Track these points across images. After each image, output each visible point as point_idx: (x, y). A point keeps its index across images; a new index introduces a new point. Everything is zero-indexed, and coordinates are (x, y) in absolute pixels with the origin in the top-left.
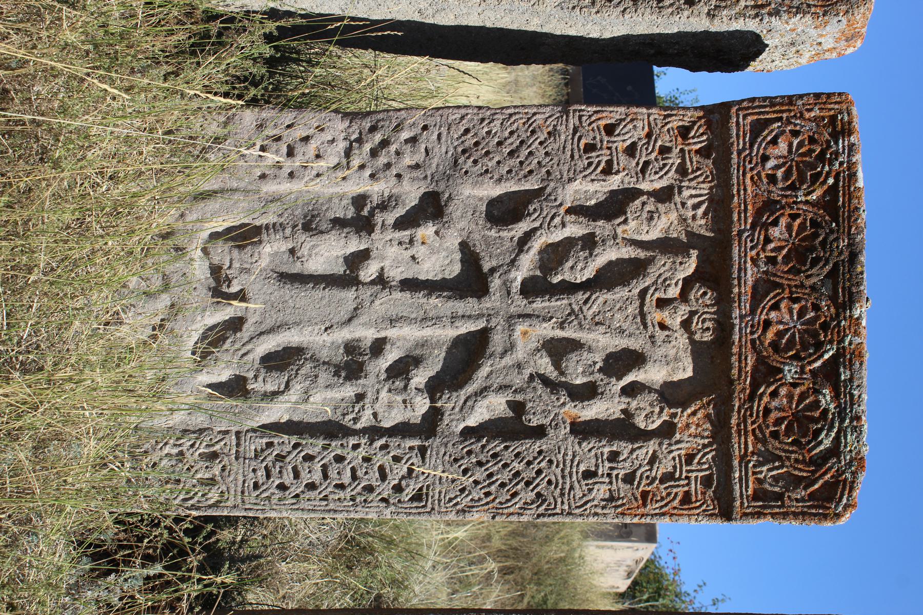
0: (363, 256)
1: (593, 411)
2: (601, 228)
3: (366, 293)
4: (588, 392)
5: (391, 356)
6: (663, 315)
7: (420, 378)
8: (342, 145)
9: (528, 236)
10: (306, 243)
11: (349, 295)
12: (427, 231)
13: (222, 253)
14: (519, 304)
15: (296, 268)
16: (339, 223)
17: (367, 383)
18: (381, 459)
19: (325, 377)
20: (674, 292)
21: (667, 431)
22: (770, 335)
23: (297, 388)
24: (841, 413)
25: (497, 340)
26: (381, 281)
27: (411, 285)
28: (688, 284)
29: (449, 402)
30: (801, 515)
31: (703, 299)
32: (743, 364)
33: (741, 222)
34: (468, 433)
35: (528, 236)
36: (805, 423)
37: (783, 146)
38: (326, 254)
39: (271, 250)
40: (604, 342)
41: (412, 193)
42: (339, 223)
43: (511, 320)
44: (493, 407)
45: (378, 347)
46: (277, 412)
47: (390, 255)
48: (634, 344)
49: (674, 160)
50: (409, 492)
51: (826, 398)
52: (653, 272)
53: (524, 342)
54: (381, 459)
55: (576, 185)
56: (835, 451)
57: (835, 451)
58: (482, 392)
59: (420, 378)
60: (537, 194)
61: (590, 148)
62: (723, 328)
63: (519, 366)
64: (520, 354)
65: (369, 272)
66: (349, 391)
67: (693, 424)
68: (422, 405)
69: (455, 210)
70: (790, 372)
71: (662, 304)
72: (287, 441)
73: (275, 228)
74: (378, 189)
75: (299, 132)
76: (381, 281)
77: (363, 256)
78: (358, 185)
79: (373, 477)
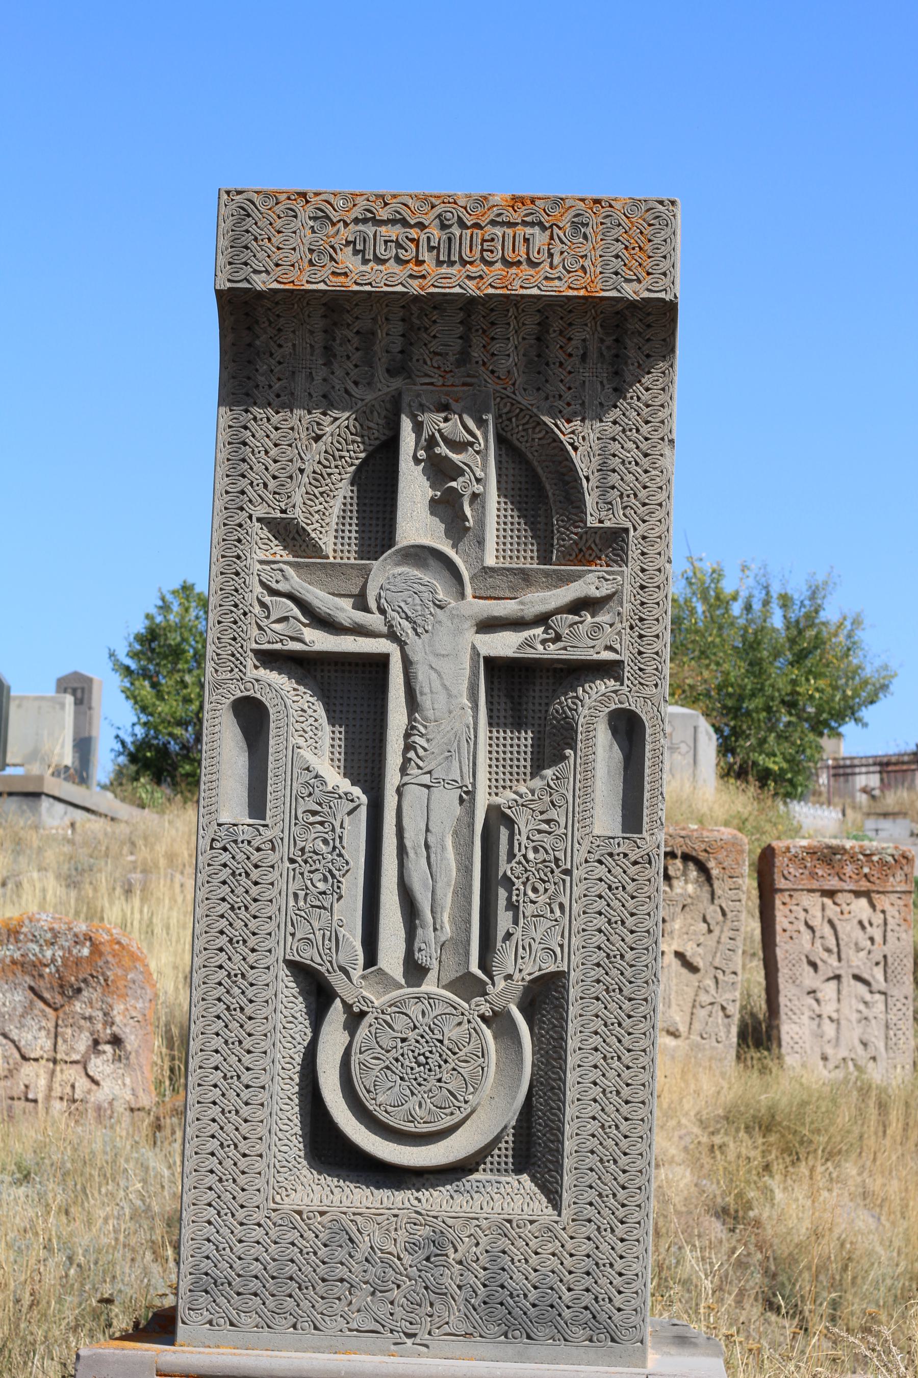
0: (830, 1018)
1: (878, 938)
2: (818, 934)
3: (842, 1017)
4: (872, 939)
5: (862, 1007)
6: (845, 912)
7: (868, 997)
8: (793, 1026)
9: (822, 960)
10: (826, 1038)
11: (843, 1022)
12: (819, 995)
13: (831, 1065)
14: (844, 963)
15: (834, 1041)
16: (819, 1026)
17: (871, 1016)
18: (895, 1009)
19: (869, 1030)
20: (838, 909)
21: (883, 912)
22: (854, 876)
23: (873, 1039)
24: (880, 853)
25: (856, 971)
26: (838, 1011)
27: (839, 1000)
28: (835, 903)
29: (875, 987)
30: (912, 867)
31: (840, 898)
32: (864, 885)
33: (815, 885)
34: (886, 980)
35: (822, 960)
36: (883, 863)
37: (791, 870)
38: (829, 1029)
39: (829, 1051)
40: (858, 934)
41: (810, 1001)
42: (819, 1026)
43: (850, 967)
44: (878, 973)
45: (860, 1012)
46: (881, 1045)
47: (829, 1009)
48: (855, 922)
49: (794, 908)
50: (904, 1001)
51: (875, 858)
52: (832, 916)
53: (858, 961)
54: (895, 1009)
55: (804, 942)
56: (893, 856)
57: (893, 856)
58: (873, 977)
59: (868, 997)
60: (807, 957)
61: (791, 938)
62: (851, 891)
63: (864, 964)
64: (860, 963)
65: (835, 1016)
66: (873, 1021)
67: (883, 902)
68: (877, 997)
69: (814, 986)
70: (866, 870)
71: (842, 913)
72: (891, 1043)
73: (821, 1047)
74: (808, 1014)
75: (789, 1040)
76: (838, 1011)
77: (830, 1018)
78: (805, 1019)
79: (900, 1013)
